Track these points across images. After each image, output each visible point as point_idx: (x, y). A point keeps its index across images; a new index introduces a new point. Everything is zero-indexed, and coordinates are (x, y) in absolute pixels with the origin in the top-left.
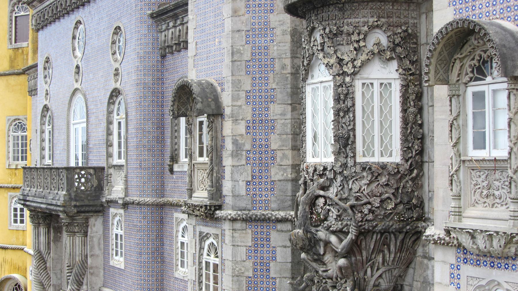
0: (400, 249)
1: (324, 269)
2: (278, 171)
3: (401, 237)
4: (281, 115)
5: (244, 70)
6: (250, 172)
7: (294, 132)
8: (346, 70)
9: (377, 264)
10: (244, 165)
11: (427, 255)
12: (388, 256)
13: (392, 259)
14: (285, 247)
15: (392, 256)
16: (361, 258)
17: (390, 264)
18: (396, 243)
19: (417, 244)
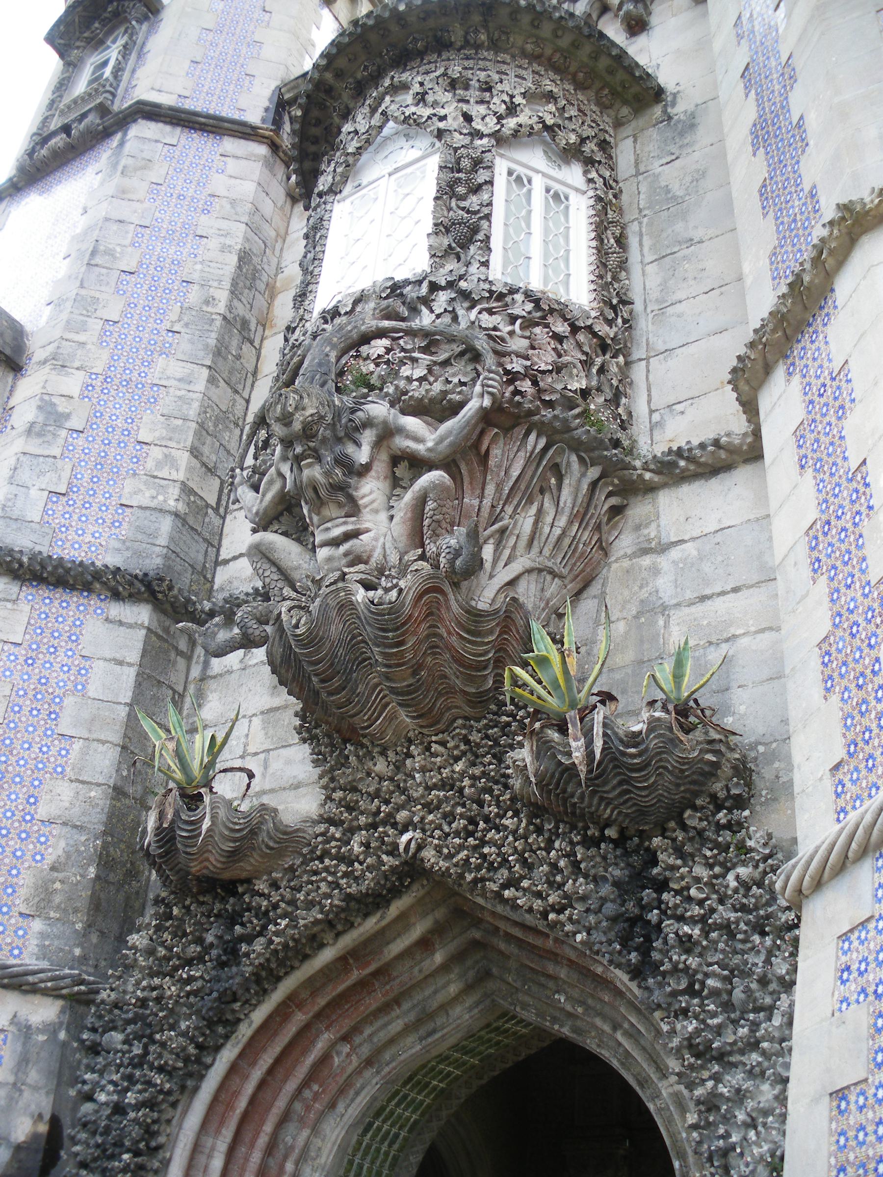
0: (585, 505)
1: (350, 527)
2: (143, 488)
3: (594, 473)
4: (180, 380)
5: (113, 285)
6: (66, 475)
7: (203, 423)
8: (478, 127)
9: (513, 539)
10: (55, 457)
11: (653, 545)
12: (549, 519)
13: (557, 531)
14: (121, 663)
15: (562, 521)
16: (476, 502)
17: (546, 552)
18: (579, 481)
19: (614, 527)
